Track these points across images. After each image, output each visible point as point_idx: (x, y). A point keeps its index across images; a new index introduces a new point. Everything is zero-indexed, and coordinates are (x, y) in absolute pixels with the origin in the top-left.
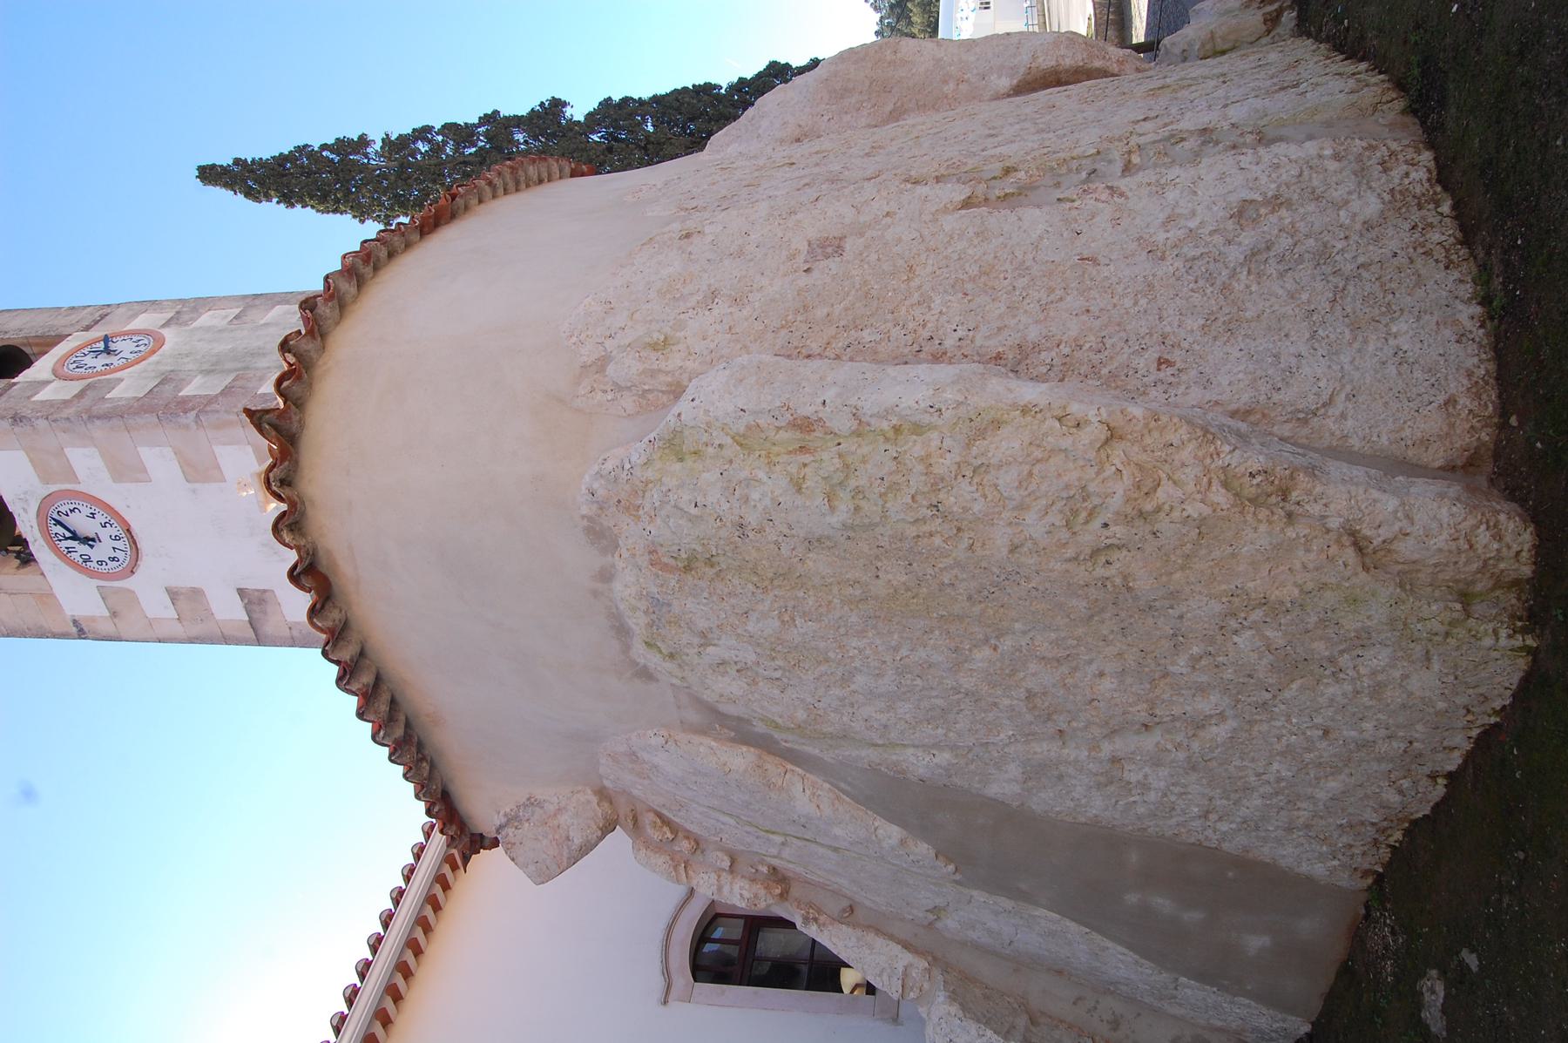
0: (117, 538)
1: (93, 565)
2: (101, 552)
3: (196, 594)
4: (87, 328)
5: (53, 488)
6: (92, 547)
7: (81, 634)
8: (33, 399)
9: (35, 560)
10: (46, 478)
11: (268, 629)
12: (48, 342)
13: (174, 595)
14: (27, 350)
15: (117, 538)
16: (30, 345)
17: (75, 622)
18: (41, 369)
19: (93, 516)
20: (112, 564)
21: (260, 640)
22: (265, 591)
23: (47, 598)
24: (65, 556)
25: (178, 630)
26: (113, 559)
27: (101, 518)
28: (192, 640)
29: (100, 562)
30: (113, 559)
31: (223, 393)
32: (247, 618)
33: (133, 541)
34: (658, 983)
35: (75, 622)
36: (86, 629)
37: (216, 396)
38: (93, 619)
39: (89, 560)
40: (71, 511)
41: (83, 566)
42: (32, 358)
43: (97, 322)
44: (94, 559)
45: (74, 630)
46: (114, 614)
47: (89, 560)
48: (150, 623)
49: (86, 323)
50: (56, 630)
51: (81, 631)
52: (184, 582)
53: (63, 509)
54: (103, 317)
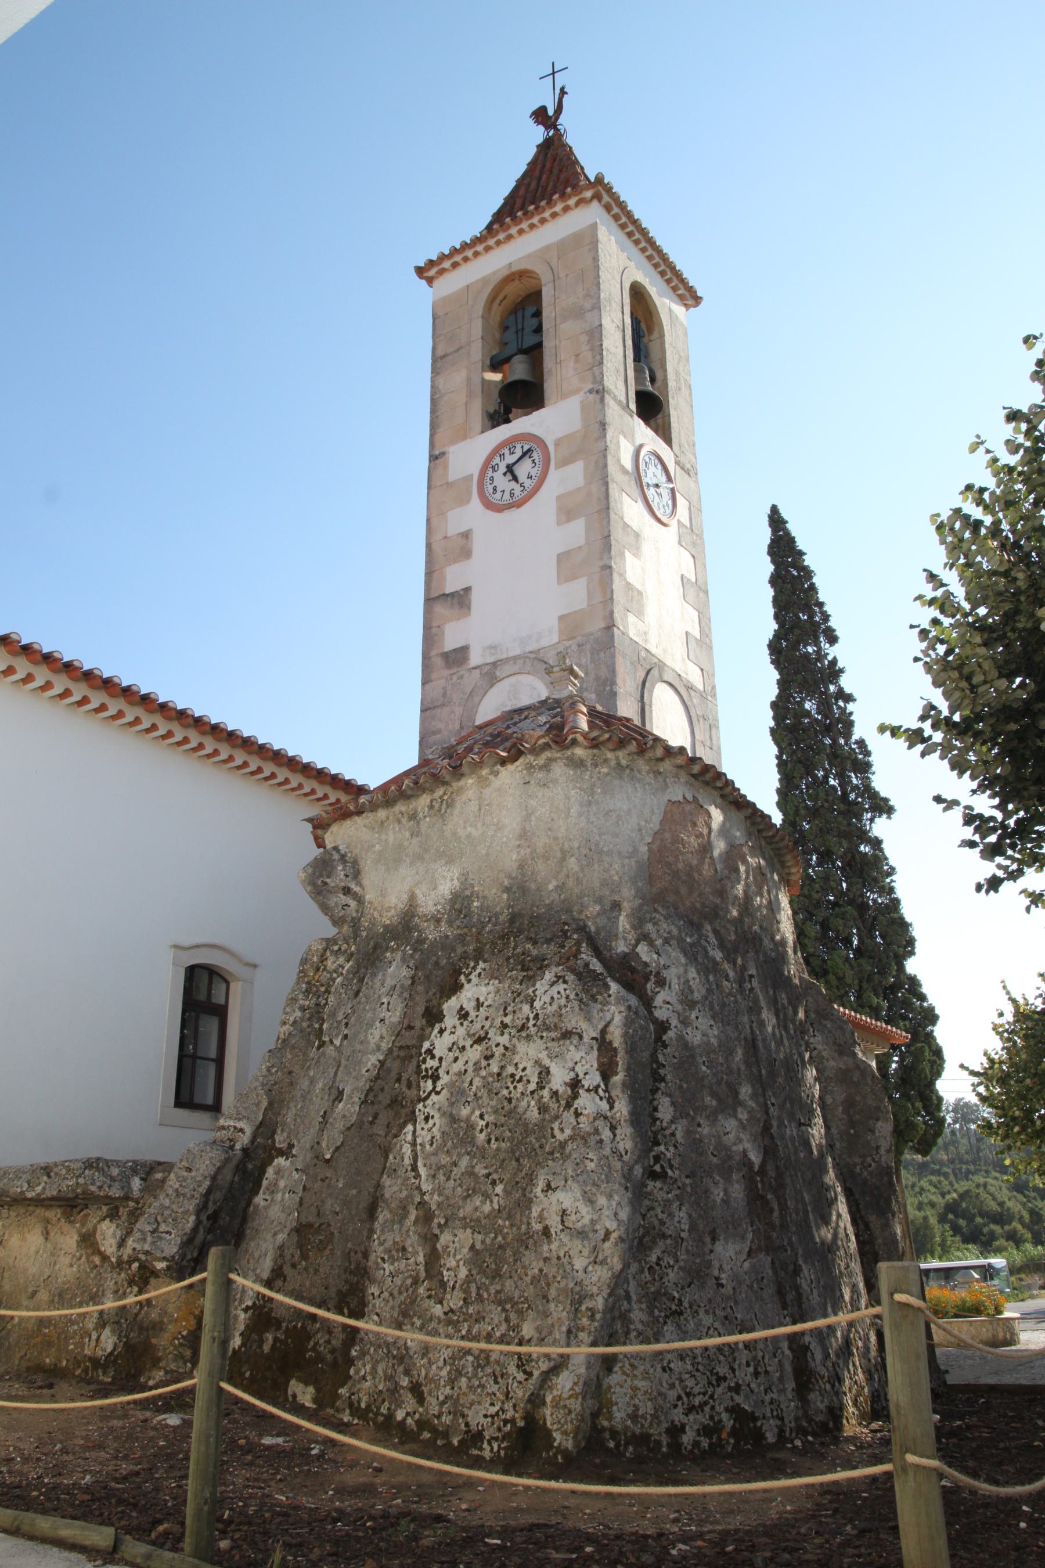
0: (512, 495)
1: (490, 473)
2: (502, 482)
3: (466, 553)
4: (677, 463)
5: (551, 448)
6: (505, 474)
7: (434, 458)
8: (622, 438)
9: (494, 427)
10: (558, 443)
11: (439, 609)
12: (665, 433)
13: (466, 535)
14: (660, 416)
15: (512, 495)
16: (663, 417)
17: (443, 454)
18: (643, 433)
19: (530, 477)
20: (490, 488)
21: (430, 601)
22: (469, 609)
23: (463, 434)
24: (497, 451)
25: (437, 537)
26: (495, 489)
27: (528, 483)
28: (429, 546)
29: (492, 479)
30: (495, 489)
31: (628, 584)
32: (447, 592)
33: (510, 506)
34: (186, 943)
35: (443, 454)
36: (437, 461)
37: (625, 579)
38: (446, 467)
39: (494, 470)
40: (533, 461)
41: (488, 465)
42: (652, 422)
43: (682, 468)
44: (495, 475)
45: (437, 453)
46: (449, 485)
47: (494, 470)
48: (443, 514)
49: (682, 459)
50: (437, 437)
51: (435, 458)
52: (478, 544)
53: (535, 455)
54: (688, 472)
